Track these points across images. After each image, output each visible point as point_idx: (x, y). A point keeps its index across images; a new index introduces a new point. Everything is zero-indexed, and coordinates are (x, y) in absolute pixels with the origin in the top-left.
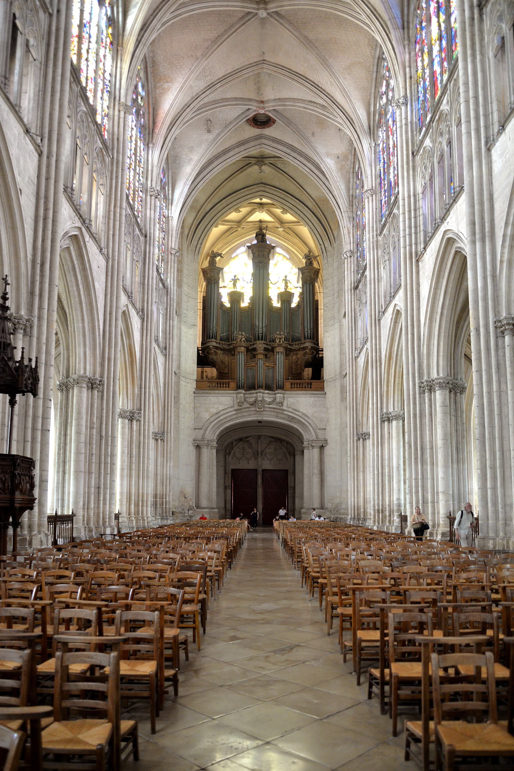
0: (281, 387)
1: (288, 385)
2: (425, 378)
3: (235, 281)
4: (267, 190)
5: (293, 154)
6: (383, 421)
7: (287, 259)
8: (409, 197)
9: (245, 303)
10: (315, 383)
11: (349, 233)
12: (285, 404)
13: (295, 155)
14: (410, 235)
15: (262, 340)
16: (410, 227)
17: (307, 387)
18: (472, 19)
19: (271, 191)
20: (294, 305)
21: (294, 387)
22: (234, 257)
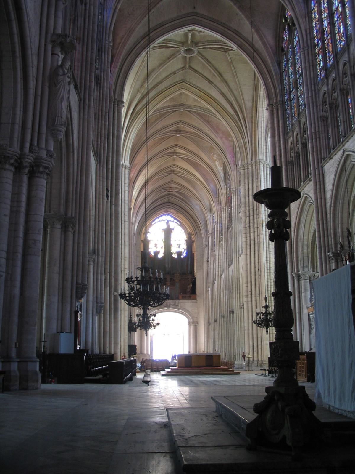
0: (178, 298)
1: (180, 296)
2: (222, 313)
3: (156, 245)
4: (170, 205)
5: (182, 202)
6: (215, 322)
7: (179, 225)
8: (218, 255)
9: (160, 256)
10: (192, 296)
11: (205, 237)
12: (179, 306)
13: (184, 202)
14: (219, 268)
15: (169, 274)
16: (218, 265)
17: (189, 298)
18: (226, 231)
19: (173, 206)
20: (182, 257)
21: (184, 298)
22: (153, 225)
